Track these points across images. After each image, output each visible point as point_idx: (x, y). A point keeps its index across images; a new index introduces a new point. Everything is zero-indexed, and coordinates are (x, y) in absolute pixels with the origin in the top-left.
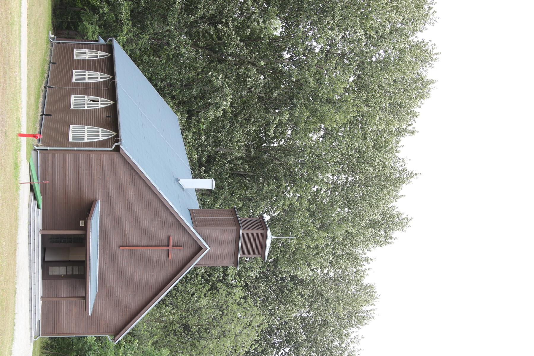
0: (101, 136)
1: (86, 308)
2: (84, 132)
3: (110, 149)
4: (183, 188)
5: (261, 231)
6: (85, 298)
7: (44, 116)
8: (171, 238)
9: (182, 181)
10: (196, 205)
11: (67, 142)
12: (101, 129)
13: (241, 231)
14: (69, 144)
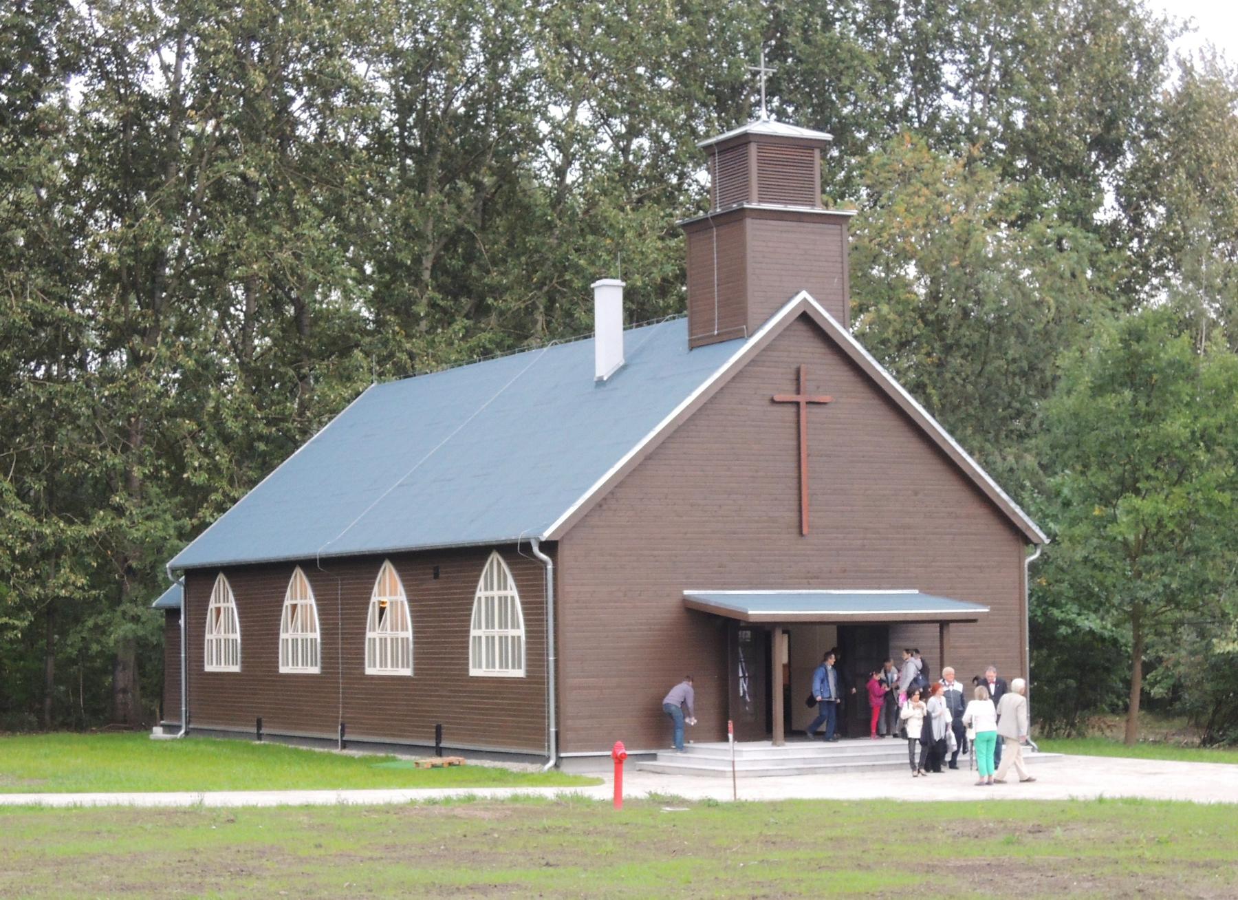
0: (502, 593)
1: (970, 620)
2: (491, 640)
3: (550, 567)
4: (624, 368)
5: (753, 149)
6: (943, 624)
7: (442, 745)
8: (777, 398)
9: (604, 368)
10: (675, 330)
11: (525, 683)
12: (481, 593)
13: (754, 205)
14: (535, 678)
